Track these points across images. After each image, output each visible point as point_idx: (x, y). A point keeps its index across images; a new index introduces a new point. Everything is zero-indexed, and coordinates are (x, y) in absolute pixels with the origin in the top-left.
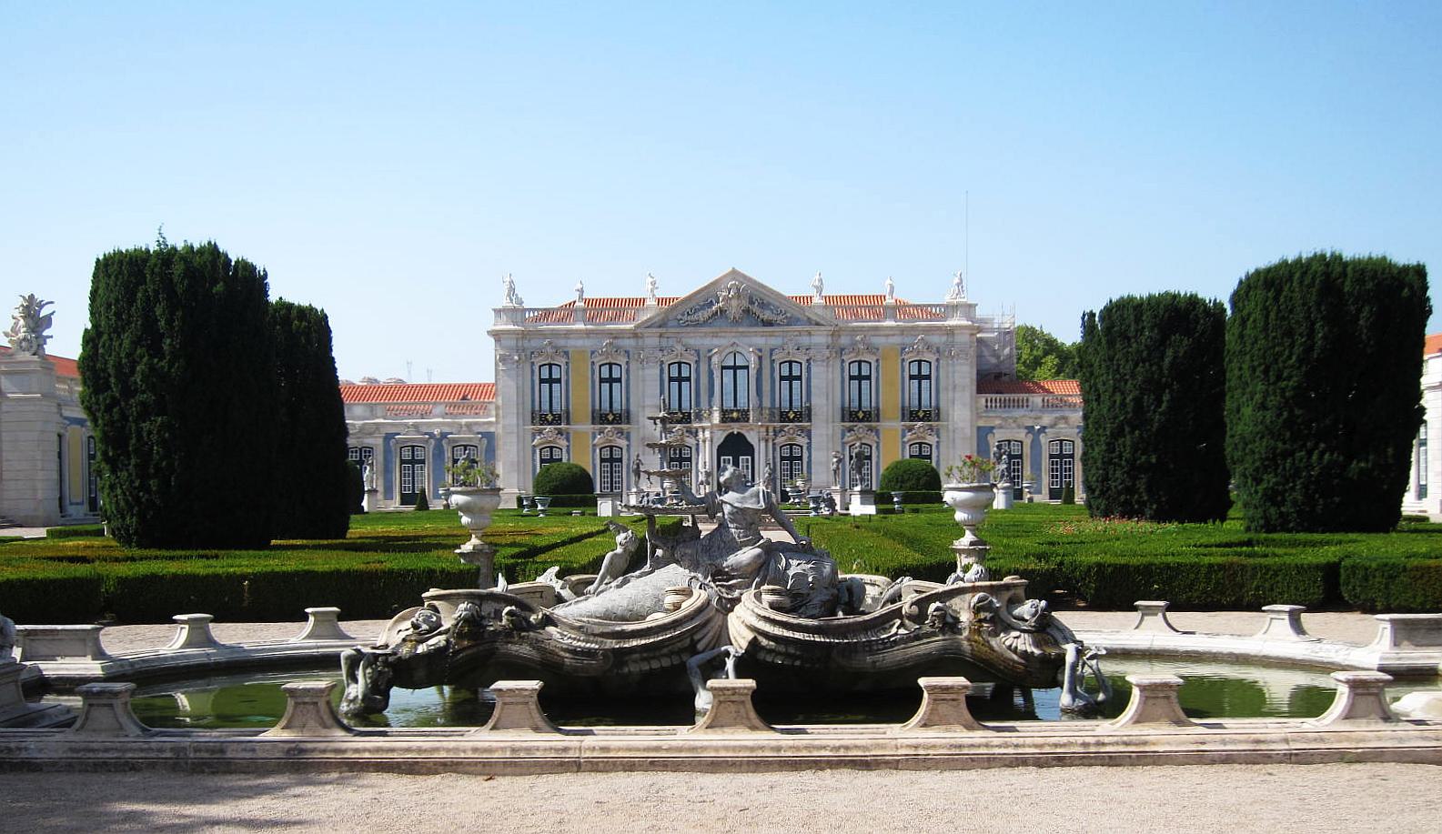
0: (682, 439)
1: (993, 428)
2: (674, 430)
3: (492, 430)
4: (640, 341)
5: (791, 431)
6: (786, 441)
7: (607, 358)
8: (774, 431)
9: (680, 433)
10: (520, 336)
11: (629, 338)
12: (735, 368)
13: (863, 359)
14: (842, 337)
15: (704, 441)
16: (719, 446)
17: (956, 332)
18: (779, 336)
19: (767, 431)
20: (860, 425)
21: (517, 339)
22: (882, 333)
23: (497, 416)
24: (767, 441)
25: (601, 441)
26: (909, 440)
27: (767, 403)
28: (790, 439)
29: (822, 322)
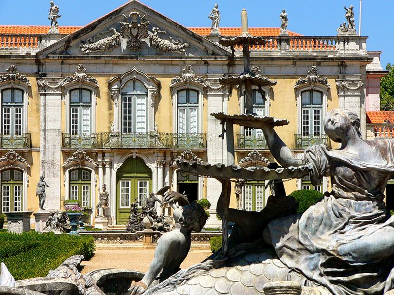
0: (83, 164)
15: (104, 166)
16: (118, 169)
17: (348, 63)
18: (178, 65)
19: (165, 156)
24: (164, 166)
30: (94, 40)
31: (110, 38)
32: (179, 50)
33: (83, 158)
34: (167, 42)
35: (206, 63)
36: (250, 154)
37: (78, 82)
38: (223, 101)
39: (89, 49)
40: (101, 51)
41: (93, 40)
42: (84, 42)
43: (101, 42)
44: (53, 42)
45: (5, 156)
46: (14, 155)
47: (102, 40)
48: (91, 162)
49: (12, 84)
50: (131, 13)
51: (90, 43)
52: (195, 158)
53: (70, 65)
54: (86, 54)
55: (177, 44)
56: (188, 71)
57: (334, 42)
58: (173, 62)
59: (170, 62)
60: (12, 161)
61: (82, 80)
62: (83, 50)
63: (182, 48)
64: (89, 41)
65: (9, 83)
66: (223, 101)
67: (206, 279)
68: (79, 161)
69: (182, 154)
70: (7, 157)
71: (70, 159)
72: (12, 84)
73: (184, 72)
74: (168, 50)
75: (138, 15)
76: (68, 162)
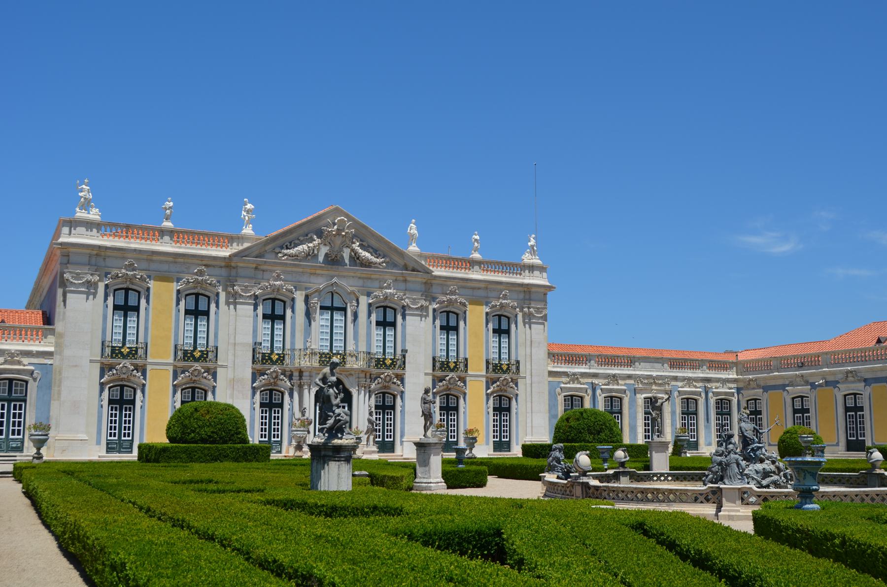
0: (275, 384)
1: (560, 382)
2: (268, 372)
3: (49, 362)
4: (233, 273)
5: (388, 379)
6: (381, 388)
7: (196, 287)
8: (370, 378)
9: (274, 376)
10: (95, 252)
11: (221, 267)
12: (332, 309)
13: (453, 310)
14: (434, 287)
15: (301, 387)
16: (317, 391)
20: (451, 375)
21: (90, 256)
22: (470, 284)
23: (57, 345)
24: (365, 387)
25: (184, 381)
26: (493, 393)
27: (363, 348)
28: (385, 387)
29: (420, 270)
30: (292, 246)
31: (311, 245)
32: (380, 264)
33: (277, 377)
34: (368, 255)
35: (405, 281)
36: (447, 378)
37: (273, 290)
38: (421, 320)
39: (286, 255)
40: (299, 258)
41: (291, 245)
42: (282, 248)
43: (300, 248)
44: (246, 245)
45: (189, 372)
46: (199, 371)
47: (301, 247)
48: (285, 382)
49: (199, 288)
50: (339, 218)
51: (287, 248)
52: (395, 381)
53: (264, 271)
54: (284, 260)
55: (377, 258)
56: (389, 287)
57: (519, 269)
58: (373, 276)
59: (369, 276)
60: (196, 378)
61: (278, 289)
62: (280, 255)
63: (382, 263)
64: (286, 246)
65: (195, 288)
66: (421, 320)
67: (563, 529)
68: (272, 381)
69: (382, 376)
70: (192, 373)
71: (263, 377)
72: (199, 288)
73: (386, 288)
74: (367, 264)
75: (345, 221)
76: (261, 381)
